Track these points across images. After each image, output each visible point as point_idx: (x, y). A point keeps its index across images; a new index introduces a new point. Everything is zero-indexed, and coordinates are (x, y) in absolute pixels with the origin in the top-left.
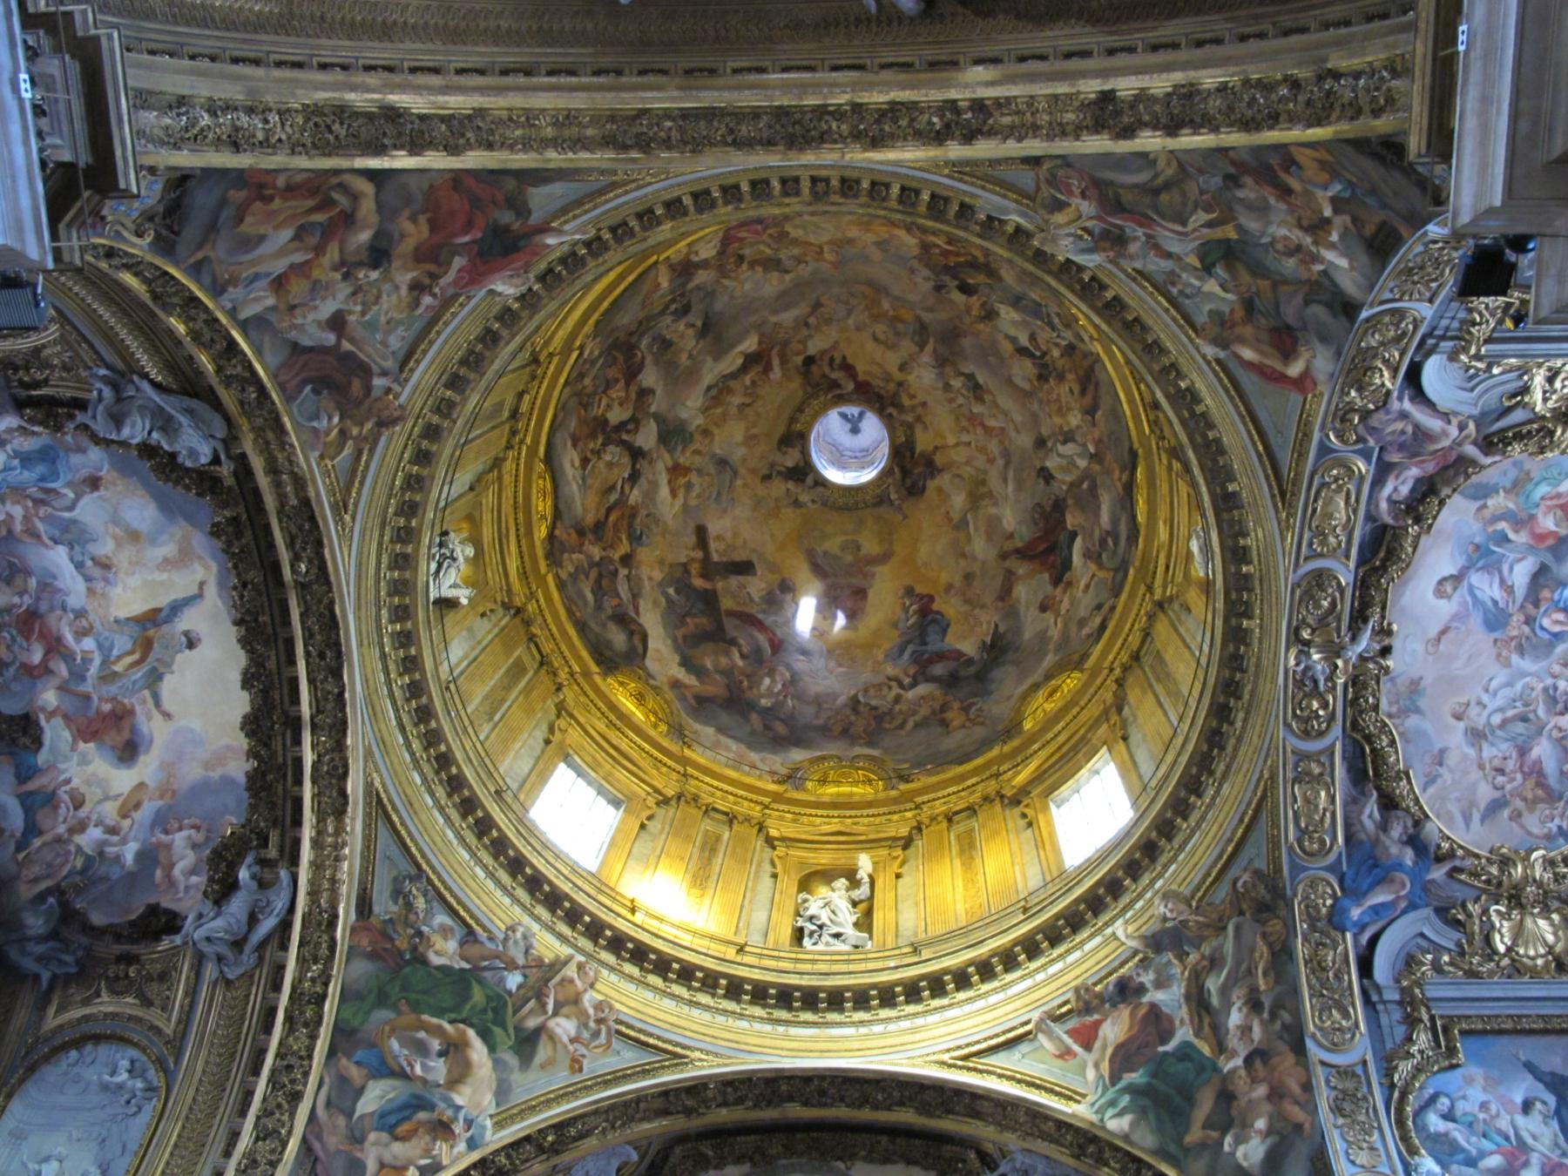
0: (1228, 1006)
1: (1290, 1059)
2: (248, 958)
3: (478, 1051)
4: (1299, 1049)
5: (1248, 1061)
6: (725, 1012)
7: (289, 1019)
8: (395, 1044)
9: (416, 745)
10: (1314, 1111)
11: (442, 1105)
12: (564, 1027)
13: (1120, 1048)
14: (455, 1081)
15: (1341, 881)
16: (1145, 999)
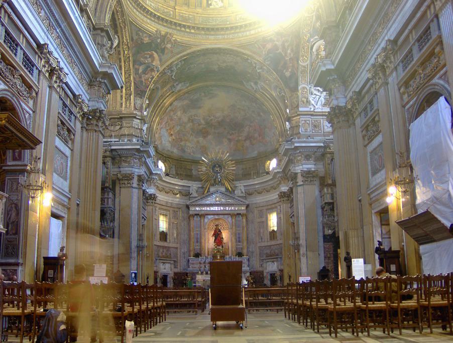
0: (288, 49)
1: (296, 62)
2: (113, 51)
3: (155, 55)
4: (298, 61)
5: (290, 59)
6: (196, 34)
7: (124, 61)
8: (142, 59)
9: (133, 4)
10: (297, 72)
11: (151, 66)
12: (169, 46)
13: (269, 50)
14: (152, 61)
15: (311, 35)
16: (275, 43)
